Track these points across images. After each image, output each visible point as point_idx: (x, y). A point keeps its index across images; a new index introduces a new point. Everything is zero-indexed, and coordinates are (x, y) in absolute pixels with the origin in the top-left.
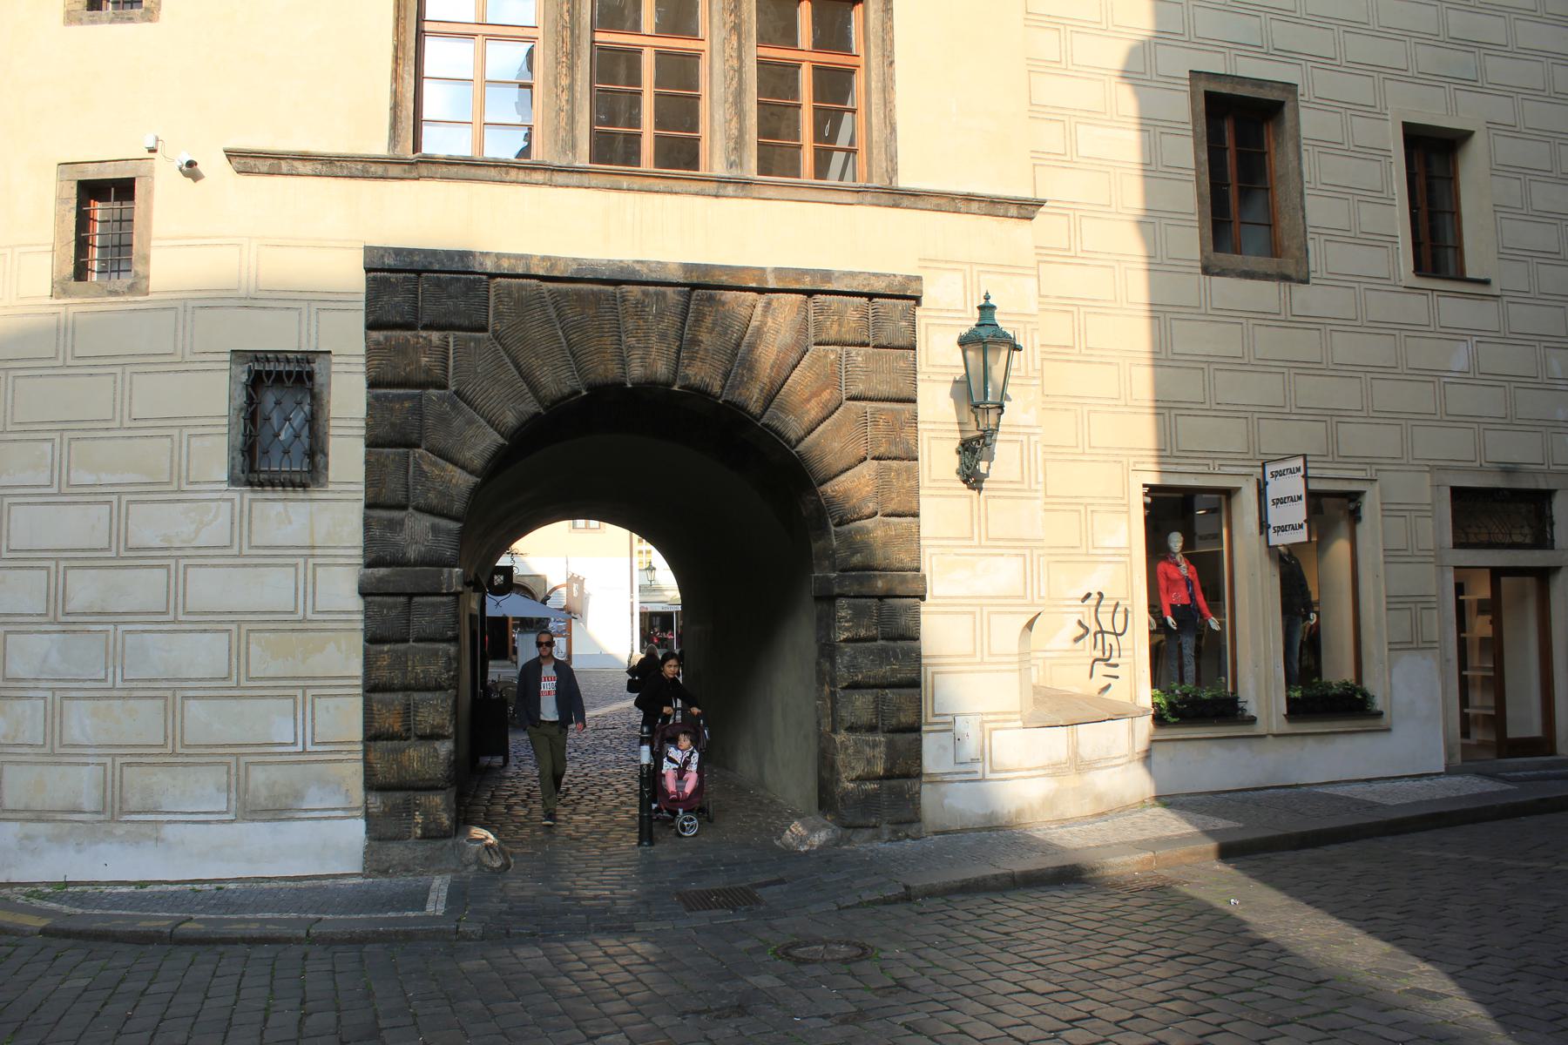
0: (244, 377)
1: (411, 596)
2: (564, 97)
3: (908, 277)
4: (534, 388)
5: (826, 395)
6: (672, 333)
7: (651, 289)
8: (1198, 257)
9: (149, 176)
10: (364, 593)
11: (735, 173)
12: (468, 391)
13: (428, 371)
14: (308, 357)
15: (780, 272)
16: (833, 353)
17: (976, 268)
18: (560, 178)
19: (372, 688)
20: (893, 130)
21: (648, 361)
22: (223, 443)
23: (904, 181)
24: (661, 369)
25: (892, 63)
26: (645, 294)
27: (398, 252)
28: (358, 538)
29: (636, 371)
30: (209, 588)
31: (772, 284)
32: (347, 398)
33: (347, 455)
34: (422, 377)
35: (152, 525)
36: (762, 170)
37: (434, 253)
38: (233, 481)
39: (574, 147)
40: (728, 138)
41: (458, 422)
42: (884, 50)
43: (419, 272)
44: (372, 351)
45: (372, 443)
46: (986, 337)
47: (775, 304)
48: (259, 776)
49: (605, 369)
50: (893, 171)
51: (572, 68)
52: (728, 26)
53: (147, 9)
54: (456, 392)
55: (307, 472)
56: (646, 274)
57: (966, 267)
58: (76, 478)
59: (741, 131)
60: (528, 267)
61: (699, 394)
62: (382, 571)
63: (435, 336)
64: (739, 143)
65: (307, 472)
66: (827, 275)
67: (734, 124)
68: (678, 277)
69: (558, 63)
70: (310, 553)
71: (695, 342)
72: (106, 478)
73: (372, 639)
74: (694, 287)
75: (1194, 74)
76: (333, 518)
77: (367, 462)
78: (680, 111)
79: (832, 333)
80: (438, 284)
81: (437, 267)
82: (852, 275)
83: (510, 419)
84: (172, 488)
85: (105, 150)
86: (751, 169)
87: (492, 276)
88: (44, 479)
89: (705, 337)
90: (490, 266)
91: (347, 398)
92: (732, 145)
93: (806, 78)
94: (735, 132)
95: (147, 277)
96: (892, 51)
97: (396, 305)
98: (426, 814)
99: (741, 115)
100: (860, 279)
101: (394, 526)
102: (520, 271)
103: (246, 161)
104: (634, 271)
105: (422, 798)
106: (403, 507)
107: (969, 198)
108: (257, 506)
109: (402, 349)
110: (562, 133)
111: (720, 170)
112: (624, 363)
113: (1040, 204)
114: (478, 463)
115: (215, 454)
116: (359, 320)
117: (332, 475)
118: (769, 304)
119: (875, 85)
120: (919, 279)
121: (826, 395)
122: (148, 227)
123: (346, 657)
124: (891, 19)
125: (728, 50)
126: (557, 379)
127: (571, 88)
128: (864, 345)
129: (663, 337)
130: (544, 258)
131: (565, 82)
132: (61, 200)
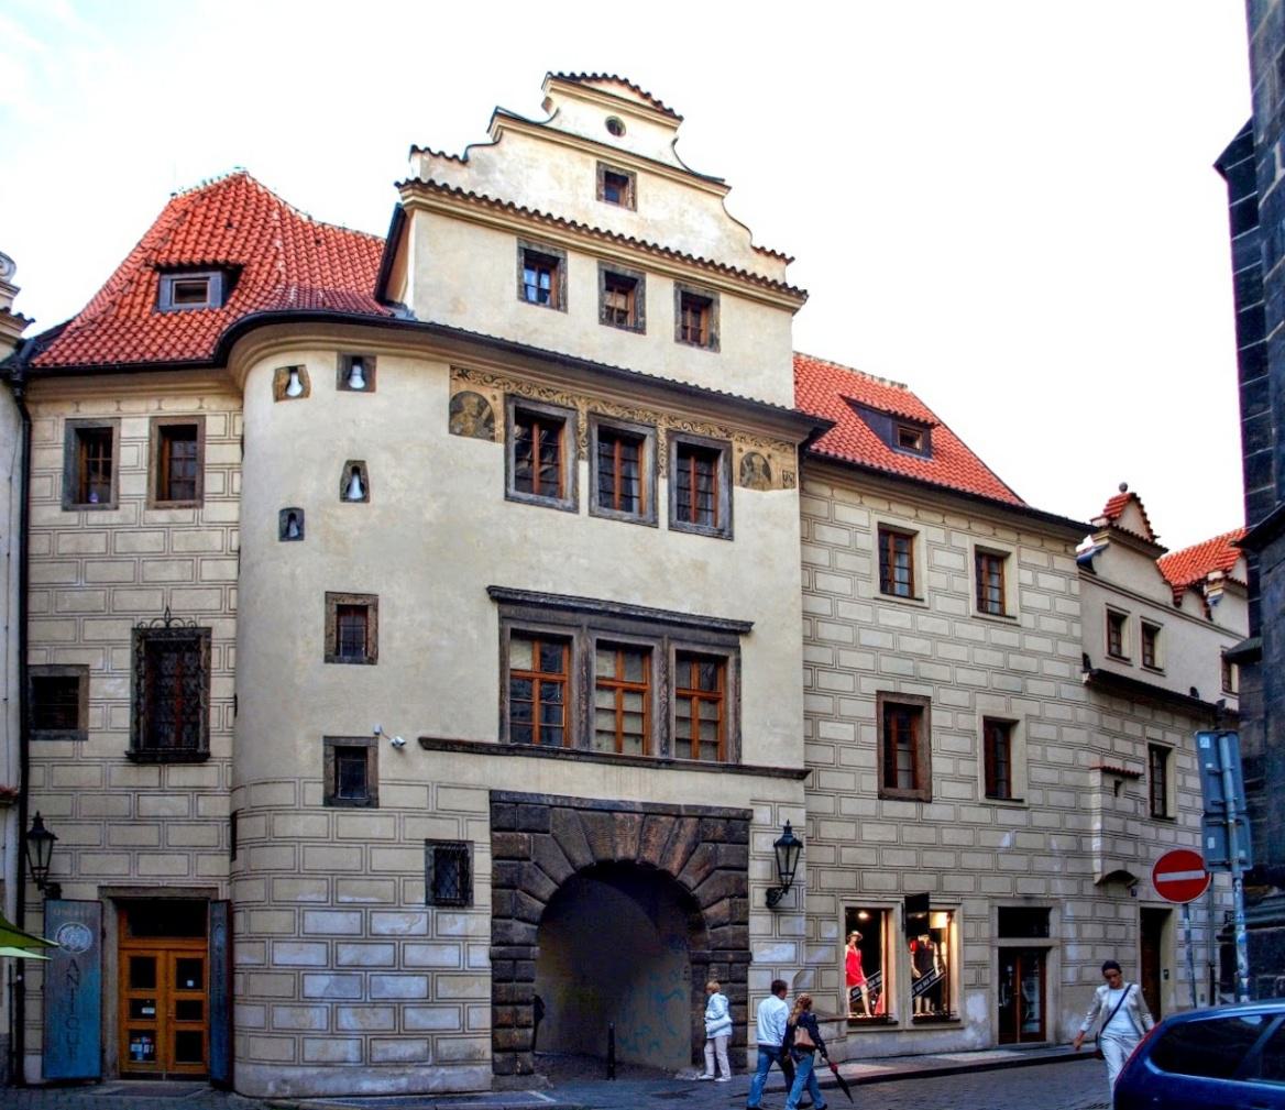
0: (432, 853)
1: (515, 960)
4: (571, 861)
5: (707, 867)
6: (637, 837)
9: (376, 747)
10: (492, 959)
11: (664, 757)
12: (542, 863)
13: (523, 852)
14: (462, 844)
15: (687, 807)
16: (711, 847)
18: (583, 758)
19: (496, 1002)
20: (740, 735)
21: (625, 849)
22: (423, 885)
23: (745, 761)
24: (632, 854)
27: (507, 793)
28: (489, 933)
29: (620, 854)
30: (414, 954)
31: (683, 812)
32: (482, 864)
33: (482, 892)
34: (520, 855)
35: (384, 924)
37: (525, 794)
38: (428, 903)
41: (537, 879)
43: (517, 804)
44: (494, 842)
45: (495, 886)
46: (788, 842)
48: (442, 1045)
49: (604, 853)
54: (536, 863)
55: (464, 900)
58: (341, 899)
59: (668, 734)
61: (649, 865)
62: (502, 948)
63: (526, 835)
65: (464, 900)
66: (709, 809)
68: (640, 809)
70: (465, 939)
71: (647, 841)
72: (357, 899)
73: (496, 980)
74: (647, 814)
76: (476, 922)
77: (493, 896)
79: (711, 837)
80: (527, 809)
82: (721, 808)
83: (562, 876)
84: (395, 905)
87: (551, 806)
88: (323, 898)
89: (653, 840)
90: (551, 801)
91: (482, 864)
94: (665, 735)
97: (504, 820)
98: (522, 1063)
101: (508, 927)
103: (428, 744)
105: (520, 1055)
106: (510, 917)
107: (775, 769)
108: (440, 917)
109: (509, 841)
112: (614, 850)
114: (547, 897)
115: (418, 891)
116: (487, 826)
117: (476, 901)
118: (681, 823)
119: (731, 710)
121: (707, 867)
123: (483, 988)
126: (583, 858)
128: (725, 842)
129: (633, 838)
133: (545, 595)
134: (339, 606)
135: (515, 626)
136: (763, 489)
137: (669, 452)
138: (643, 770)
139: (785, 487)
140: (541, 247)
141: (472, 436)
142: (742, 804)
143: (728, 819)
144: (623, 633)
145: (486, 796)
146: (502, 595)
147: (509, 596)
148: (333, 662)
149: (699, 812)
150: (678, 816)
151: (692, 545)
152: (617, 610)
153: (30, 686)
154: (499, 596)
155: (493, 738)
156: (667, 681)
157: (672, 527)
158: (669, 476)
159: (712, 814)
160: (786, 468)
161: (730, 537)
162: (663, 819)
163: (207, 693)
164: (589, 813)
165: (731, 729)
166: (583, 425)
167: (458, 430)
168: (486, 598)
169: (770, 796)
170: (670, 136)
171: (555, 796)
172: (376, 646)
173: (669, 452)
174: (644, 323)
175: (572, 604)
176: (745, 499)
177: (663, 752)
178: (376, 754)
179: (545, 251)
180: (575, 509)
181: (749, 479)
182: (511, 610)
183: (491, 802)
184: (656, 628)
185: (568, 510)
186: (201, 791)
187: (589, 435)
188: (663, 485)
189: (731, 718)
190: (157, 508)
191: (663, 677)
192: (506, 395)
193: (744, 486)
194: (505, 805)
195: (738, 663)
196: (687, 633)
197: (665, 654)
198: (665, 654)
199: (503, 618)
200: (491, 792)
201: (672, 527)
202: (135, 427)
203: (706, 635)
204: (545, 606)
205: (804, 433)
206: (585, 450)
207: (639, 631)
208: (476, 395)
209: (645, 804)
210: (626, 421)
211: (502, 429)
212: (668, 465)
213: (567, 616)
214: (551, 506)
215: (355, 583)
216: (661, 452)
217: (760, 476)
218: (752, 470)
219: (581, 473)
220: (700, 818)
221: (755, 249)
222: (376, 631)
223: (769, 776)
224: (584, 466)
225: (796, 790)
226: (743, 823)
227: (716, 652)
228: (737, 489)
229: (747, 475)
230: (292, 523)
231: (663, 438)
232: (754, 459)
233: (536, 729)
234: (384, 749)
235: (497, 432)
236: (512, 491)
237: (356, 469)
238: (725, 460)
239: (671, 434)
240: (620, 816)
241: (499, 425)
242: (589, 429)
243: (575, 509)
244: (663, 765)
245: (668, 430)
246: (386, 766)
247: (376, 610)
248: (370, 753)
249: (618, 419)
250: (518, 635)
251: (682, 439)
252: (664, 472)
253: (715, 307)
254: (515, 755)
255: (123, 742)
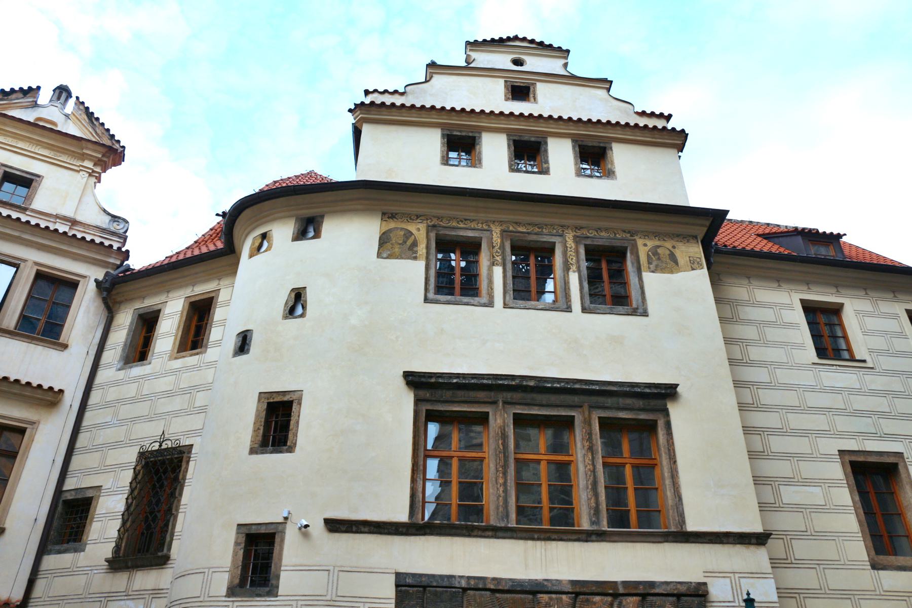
2: (501, 489)
3: (699, 584)
7: (554, 596)
8: (867, 558)
9: (283, 532)
11: (595, 528)
15: (625, 583)
17: (737, 575)
18: (500, 534)
20: (680, 499)
25: (675, 462)
26: (551, 599)
31: (621, 590)
36: (611, 524)
37: (433, 576)
39: (507, 516)
40: (590, 508)
42: (670, 455)
43: (425, 587)
47: (624, 603)
50: (683, 522)
51: (505, 474)
52: (586, 448)
53: (290, 447)
56: (550, 587)
57: (731, 575)
60: (485, 584)
64: (597, 511)
66: (652, 584)
67: (593, 501)
68: (568, 588)
69: (497, 471)
74: (577, 594)
75: (842, 452)
78: (563, 493)
81: (435, 584)
85: (261, 514)
86: (604, 526)
87: (465, 590)
90: (464, 584)
92: (592, 512)
93: (628, 471)
94: (593, 505)
95: (277, 587)
96: (675, 455)
99: (596, 495)
100: (671, 586)
102: (481, 586)
103: (334, 526)
104: (544, 586)
110: (501, 509)
111: (586, 525)
113: (771, 534)
118: (620, 603)
119: (667, 474)
120: (705, 584)
122: (280, 559)
124: (672, 438)
125: (587, 461)
127: (505, 484)
130: (494, 579)
131: (501, 481)
132: (237, 544)
133: (458, 376)
134: (268, 403)
135: (430, 407)
136: (672, 272)
137: (577, 252)
138: (570, 544)
139: (693, 269)
140: (460, 131)
141: (397, 258)
142: (693, 576)
143: (679, 596)
144: (541, 405)
145: (392, 578)
146: (416, 379)
147: (423, 380)
148: (257, 453)
149: (641, 590)
150: (616, 595)
151: (610, 323)
152: (532, 383)
153: (60, 508)
154: (416, 381)
155: (403, 516)
156: (591, 449)
157: (584, 310)
158: (579, 271)
159: (657, 591)
160: (692, 255)
161: (645, 314)
162: (597, 598)
163: (179, 501)
164: (508, 596)
165: (669, 494)
166: (497, 238)
167: (385, 255)
168: (401, 382)
169: (725, 566)
170: (563, 61)
171: (469, 578)
172: (296, 435)
173: (577, 252)
174: (548, 168)
175: (485, 381)
176: (655, 285)
177: (592, 523)
178: (282, 540)
179: (464, 134)
180: (490, 304)
181: (657, 266)
182: (427, 394)
183: (397, 586)
184: (576, 399)
185: (485, 305)
186: (157, 593)
187: (502, 247)
188: (574, 278)
189: (668, 482)
190: (176, 358)
191: (587, 444)
192: (428, 226)
193: (653, 272)
194: (411, 590)
195: (668, 425)
196: (609, 401)
197: (588, 422)
198: (588, 422)
199: (418, 401)
200: (398, 575)
201: (584, 310)
202: (173, 311)
203: (629, 401)
204: (459, 387)
205: (702, 225)
206: (499, 259)
207: (558, 403)
208: (402, 229)
209: (574, 583)
210: (536, 234)
211: (425, 251)
212: (578, 261)
213: (481, 395)
214: (467, 304)
215: (280, 383)
216: (569, 253)
217: (670, 264)
218: (659, 259)
219: (496, 276)
220: (644, 596)
221: (637, 113)
222: (298, 422)
223: (721, 543)
224: (498, 271)
225: (758, 557)
226: (696, 600)
227: (643, 416)
228: (647, 276)
229: (655, 263)
230: (244, 344)
231: (570, 243)
232: (660, 251)
233: (454, 509)
234: (291, 536)
235: (419, 253)
236: (431, 295)
237: (298, 296)
238: (632, 253)
239: (577, 240)
240: (544, 597)
241: (422, 249)
242: (502, 243)
243: (490, 304)
244: (594, 537)
245: (575, 237)
246: (290, 552)
247: (300, 404)
248: (277, 539)
249: (528, 233)
250: (432, 416)
251: (588, 242)
252: (574, 268)
253: (609, 152)
254: (424, 534)
255: (107, 550)
